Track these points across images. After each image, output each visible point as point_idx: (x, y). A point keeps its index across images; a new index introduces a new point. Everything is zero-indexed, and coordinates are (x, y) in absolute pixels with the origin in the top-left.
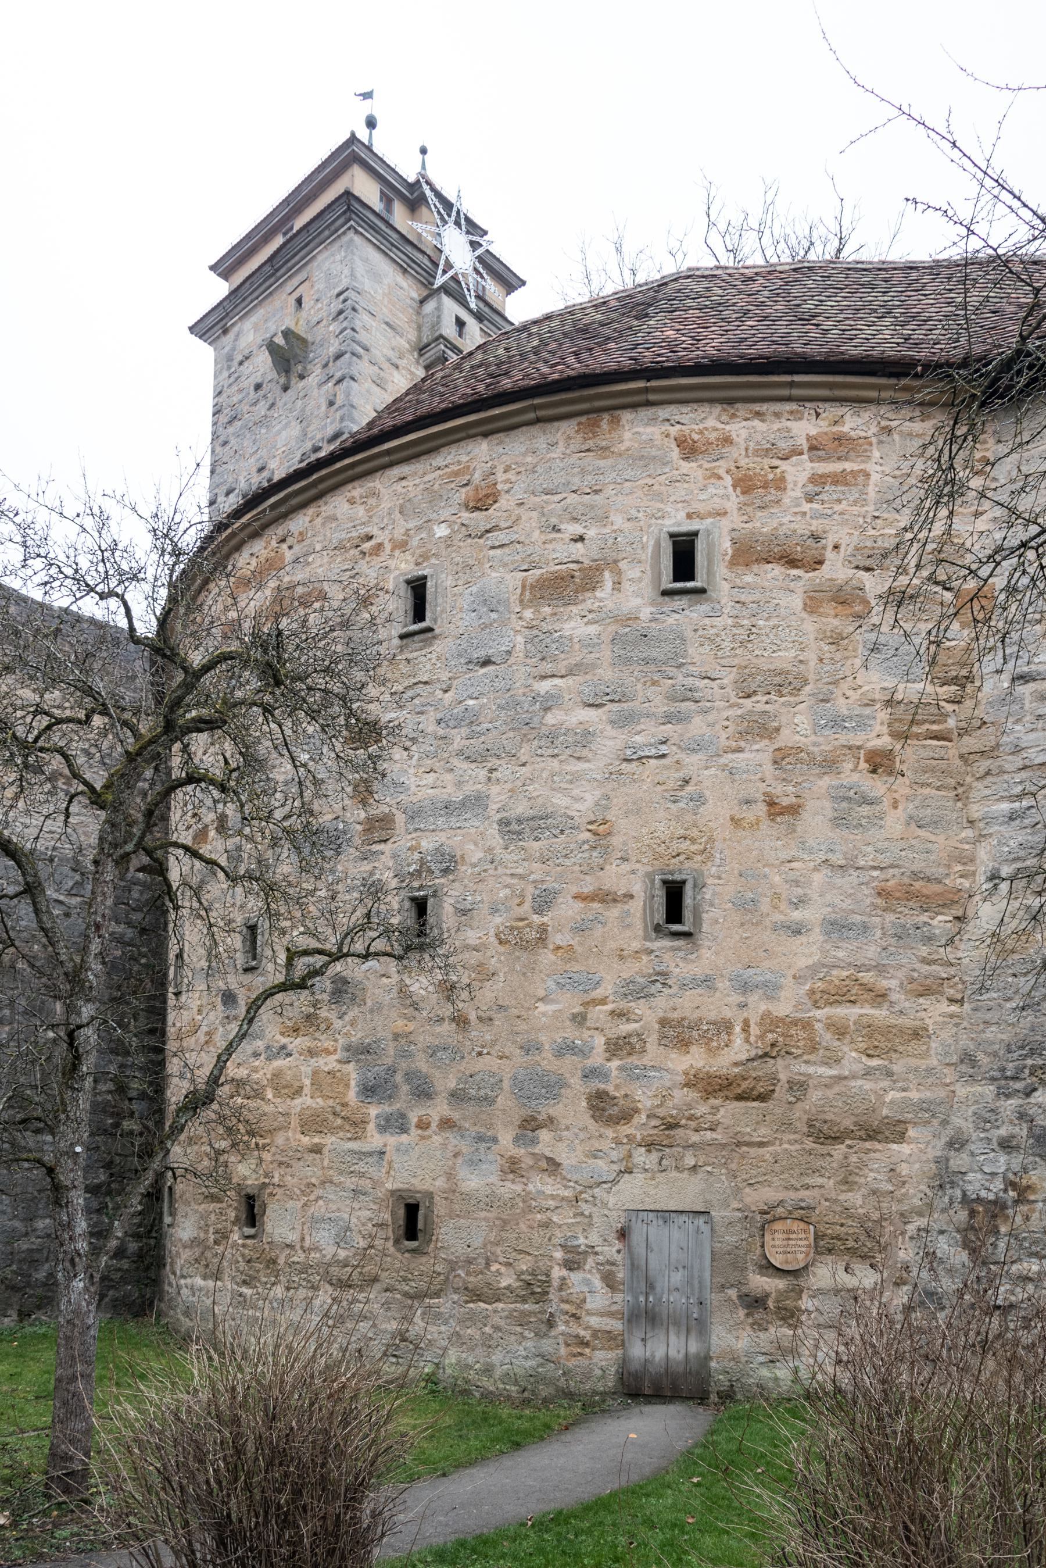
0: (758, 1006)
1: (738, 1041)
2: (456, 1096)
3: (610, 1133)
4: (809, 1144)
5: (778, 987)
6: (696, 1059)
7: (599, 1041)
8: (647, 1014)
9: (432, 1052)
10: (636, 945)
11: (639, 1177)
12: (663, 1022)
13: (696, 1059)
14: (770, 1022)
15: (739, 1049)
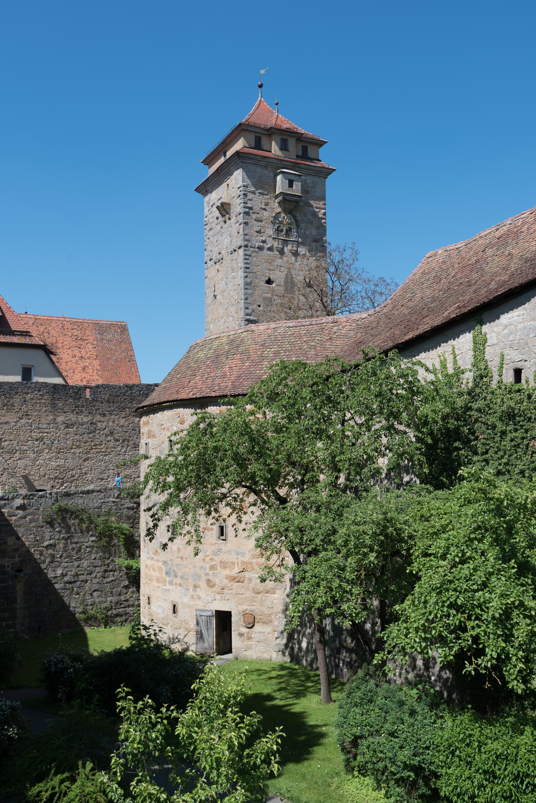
0: (241, 559)
1: (236, 568)
2: (181, 577)
3: (210, 590)
4: (253, 594)
5: (245, 553)
6: (227, 572)
7: (208, 566)
8: (217, 559)
9: (177, 565)
10: (215, 542)
11: (217, 601)
12: (221, 562)
13: (227, 572)
14: (243, 563)
15: (237, 570)
